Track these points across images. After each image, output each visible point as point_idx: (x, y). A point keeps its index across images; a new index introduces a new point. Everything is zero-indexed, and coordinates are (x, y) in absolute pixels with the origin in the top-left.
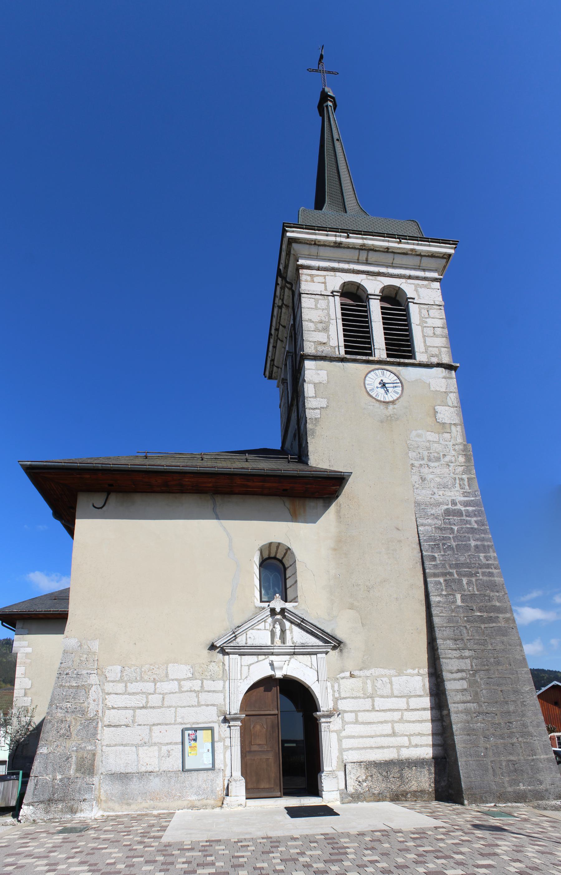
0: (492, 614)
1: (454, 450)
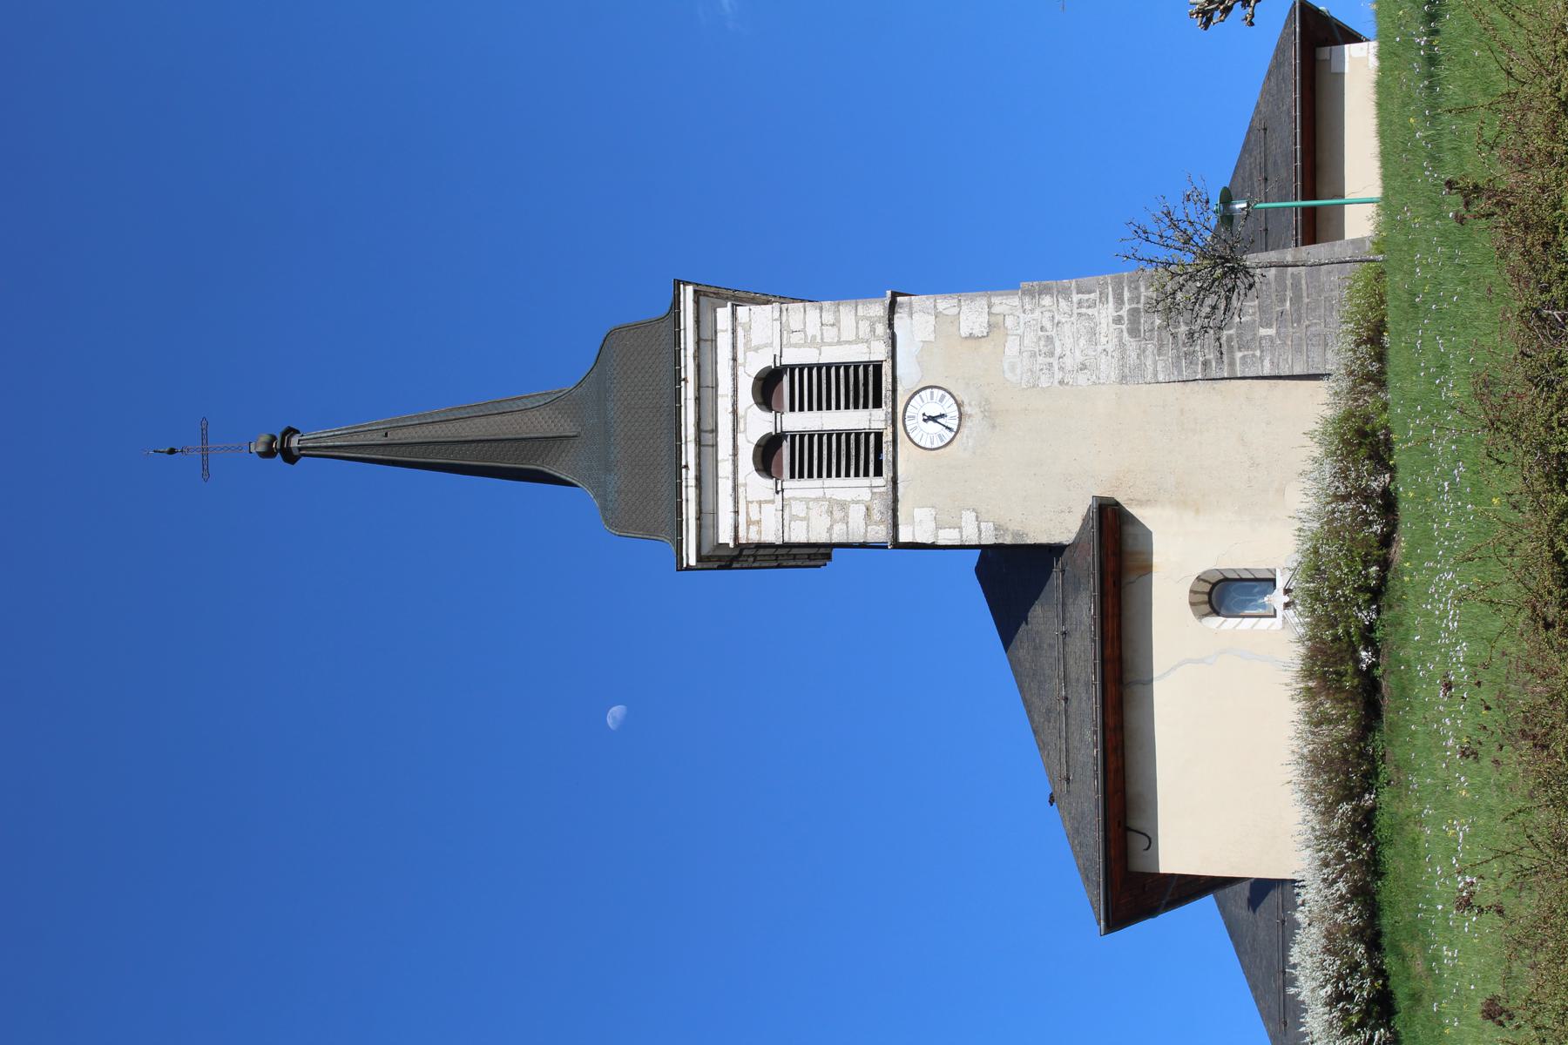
0: (1289, 283)
1: (1032, 311)
